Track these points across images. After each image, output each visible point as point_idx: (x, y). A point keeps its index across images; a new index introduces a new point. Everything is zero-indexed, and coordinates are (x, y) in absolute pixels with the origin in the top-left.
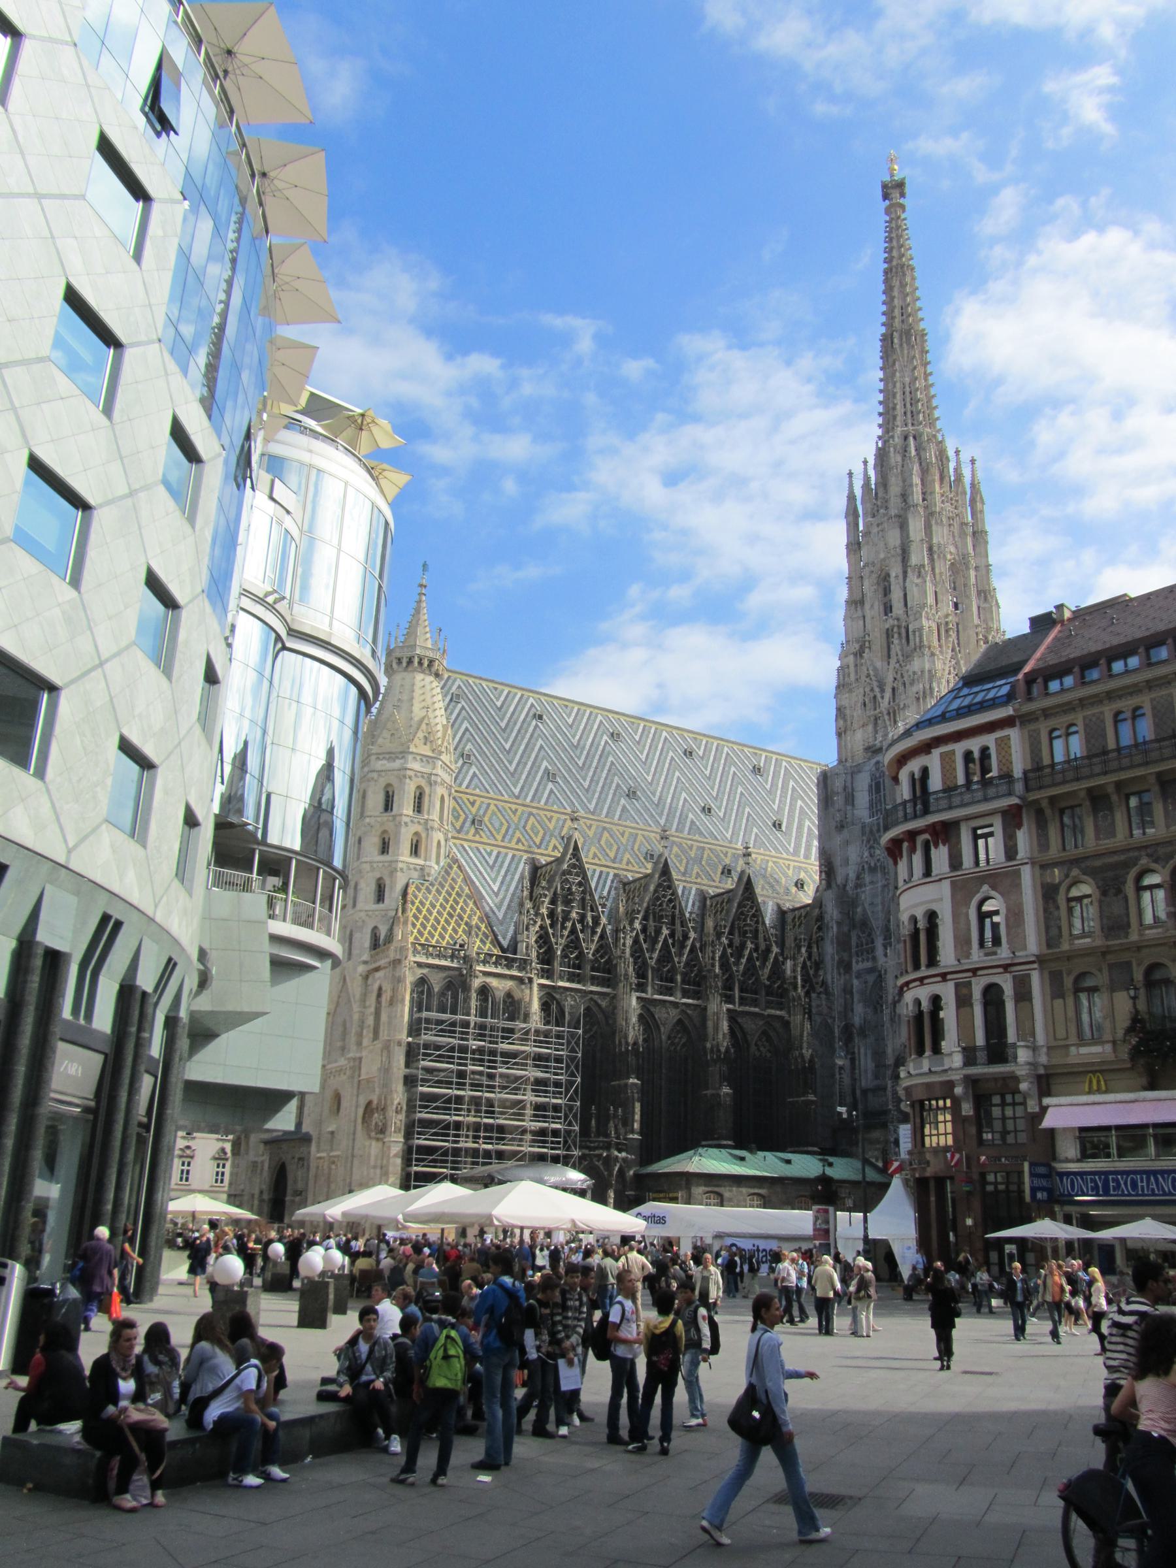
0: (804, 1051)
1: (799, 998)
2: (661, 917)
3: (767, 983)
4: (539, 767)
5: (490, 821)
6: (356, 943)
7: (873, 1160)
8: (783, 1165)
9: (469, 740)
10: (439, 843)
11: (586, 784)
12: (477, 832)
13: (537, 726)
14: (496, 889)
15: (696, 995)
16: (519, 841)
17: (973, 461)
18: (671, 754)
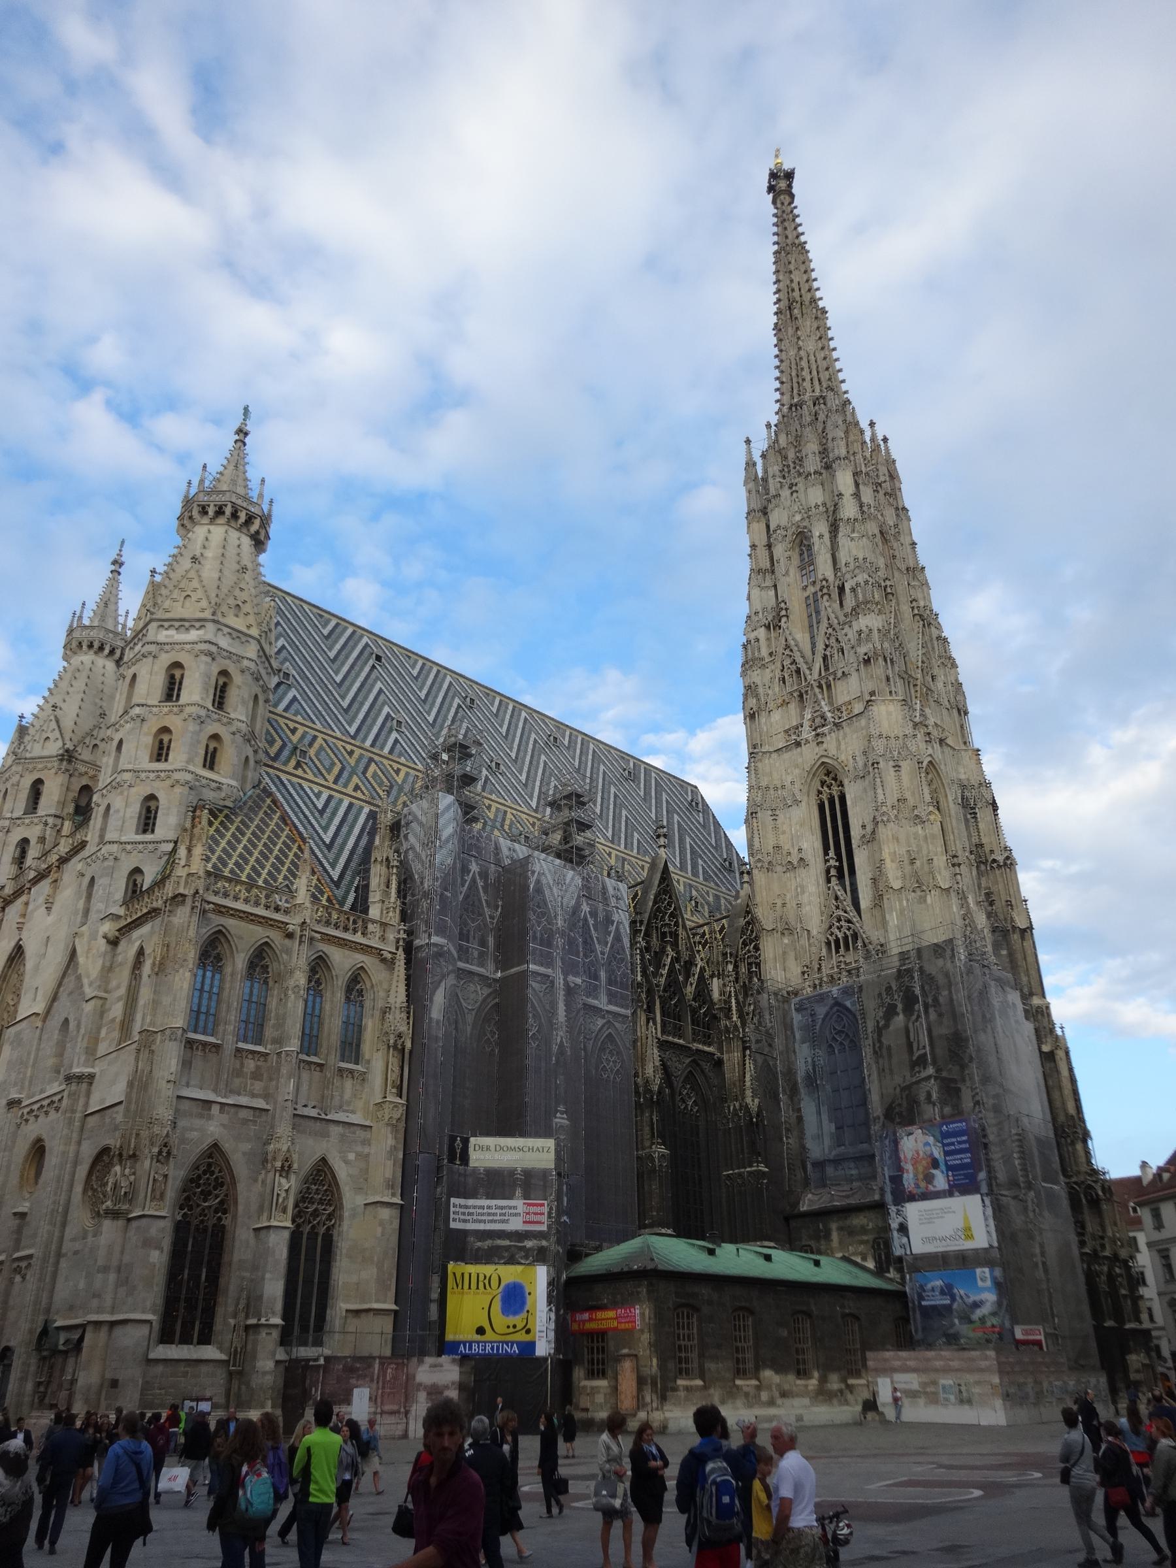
0: (749, 1100)
1: (736, 1025)
4: (380, 711)
5: (317, 755)
6: (98, 891)
7: (859, 1260)
8: (762, 1261)
9: (286, 659)
10: (247, 758)
12: (298, 765)
13: (373, 667)
14: (328, 841)
16: (357, 788)
17: (885, 440)
18: (533, 736)
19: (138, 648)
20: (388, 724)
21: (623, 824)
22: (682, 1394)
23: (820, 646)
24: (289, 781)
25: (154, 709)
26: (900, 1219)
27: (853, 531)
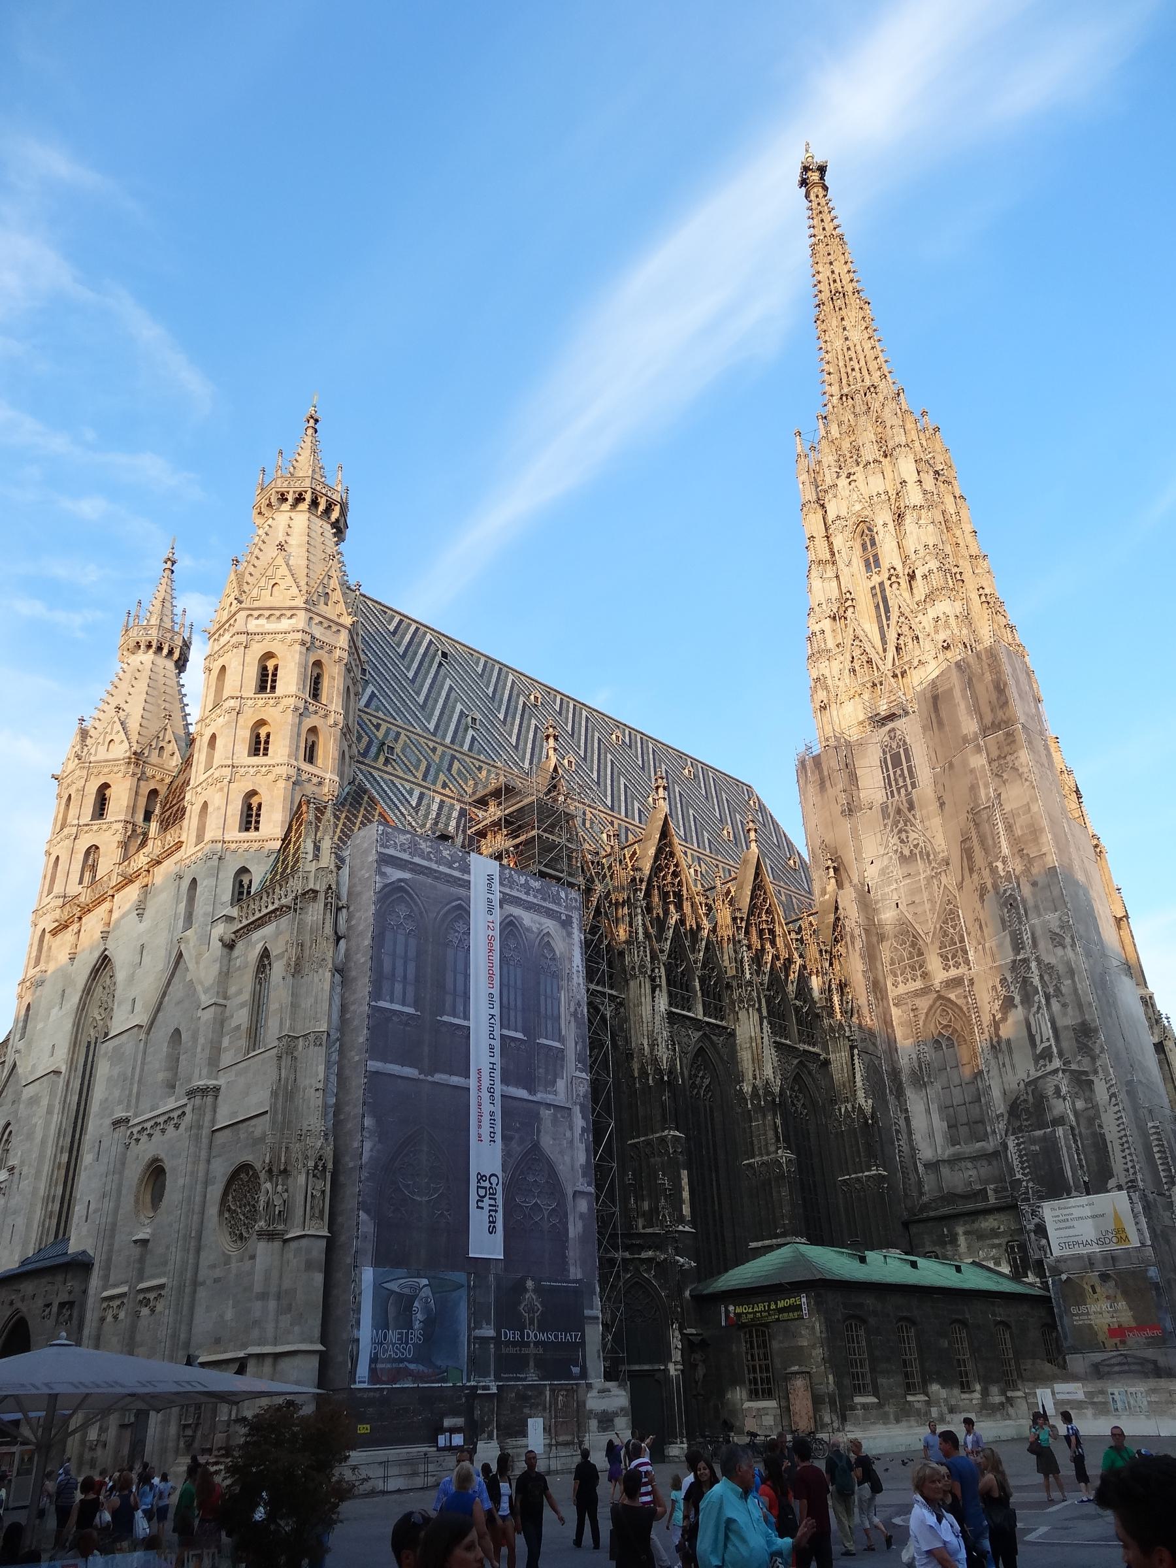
0: (861, 1100)
2: (666, 894)
3: (798, 1003)
4: (454, 707)
5: (403, 751)
7: (991, 1265)
8: (908, 1267)
11: (514, 741)
12: (387, 761)
13: (440, 664)
15: (719, 1012)
16: (445, 786)
19: (227, 637)
20: (463, 721)
21: (692, 823)
22: (860, 1412)
23: (891, 636)
24: (381, 777)
25: (250, 702)
26: (1037, 1220)
27: (919, 518)
